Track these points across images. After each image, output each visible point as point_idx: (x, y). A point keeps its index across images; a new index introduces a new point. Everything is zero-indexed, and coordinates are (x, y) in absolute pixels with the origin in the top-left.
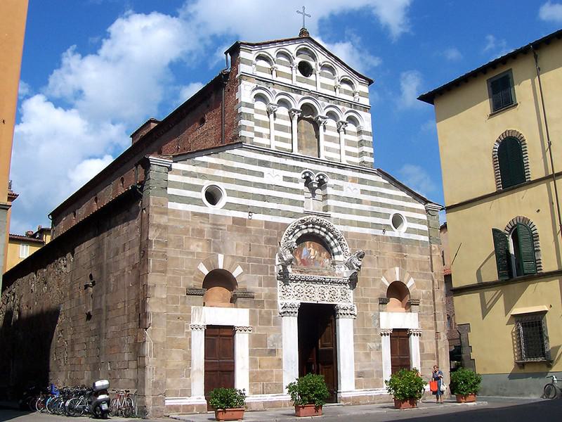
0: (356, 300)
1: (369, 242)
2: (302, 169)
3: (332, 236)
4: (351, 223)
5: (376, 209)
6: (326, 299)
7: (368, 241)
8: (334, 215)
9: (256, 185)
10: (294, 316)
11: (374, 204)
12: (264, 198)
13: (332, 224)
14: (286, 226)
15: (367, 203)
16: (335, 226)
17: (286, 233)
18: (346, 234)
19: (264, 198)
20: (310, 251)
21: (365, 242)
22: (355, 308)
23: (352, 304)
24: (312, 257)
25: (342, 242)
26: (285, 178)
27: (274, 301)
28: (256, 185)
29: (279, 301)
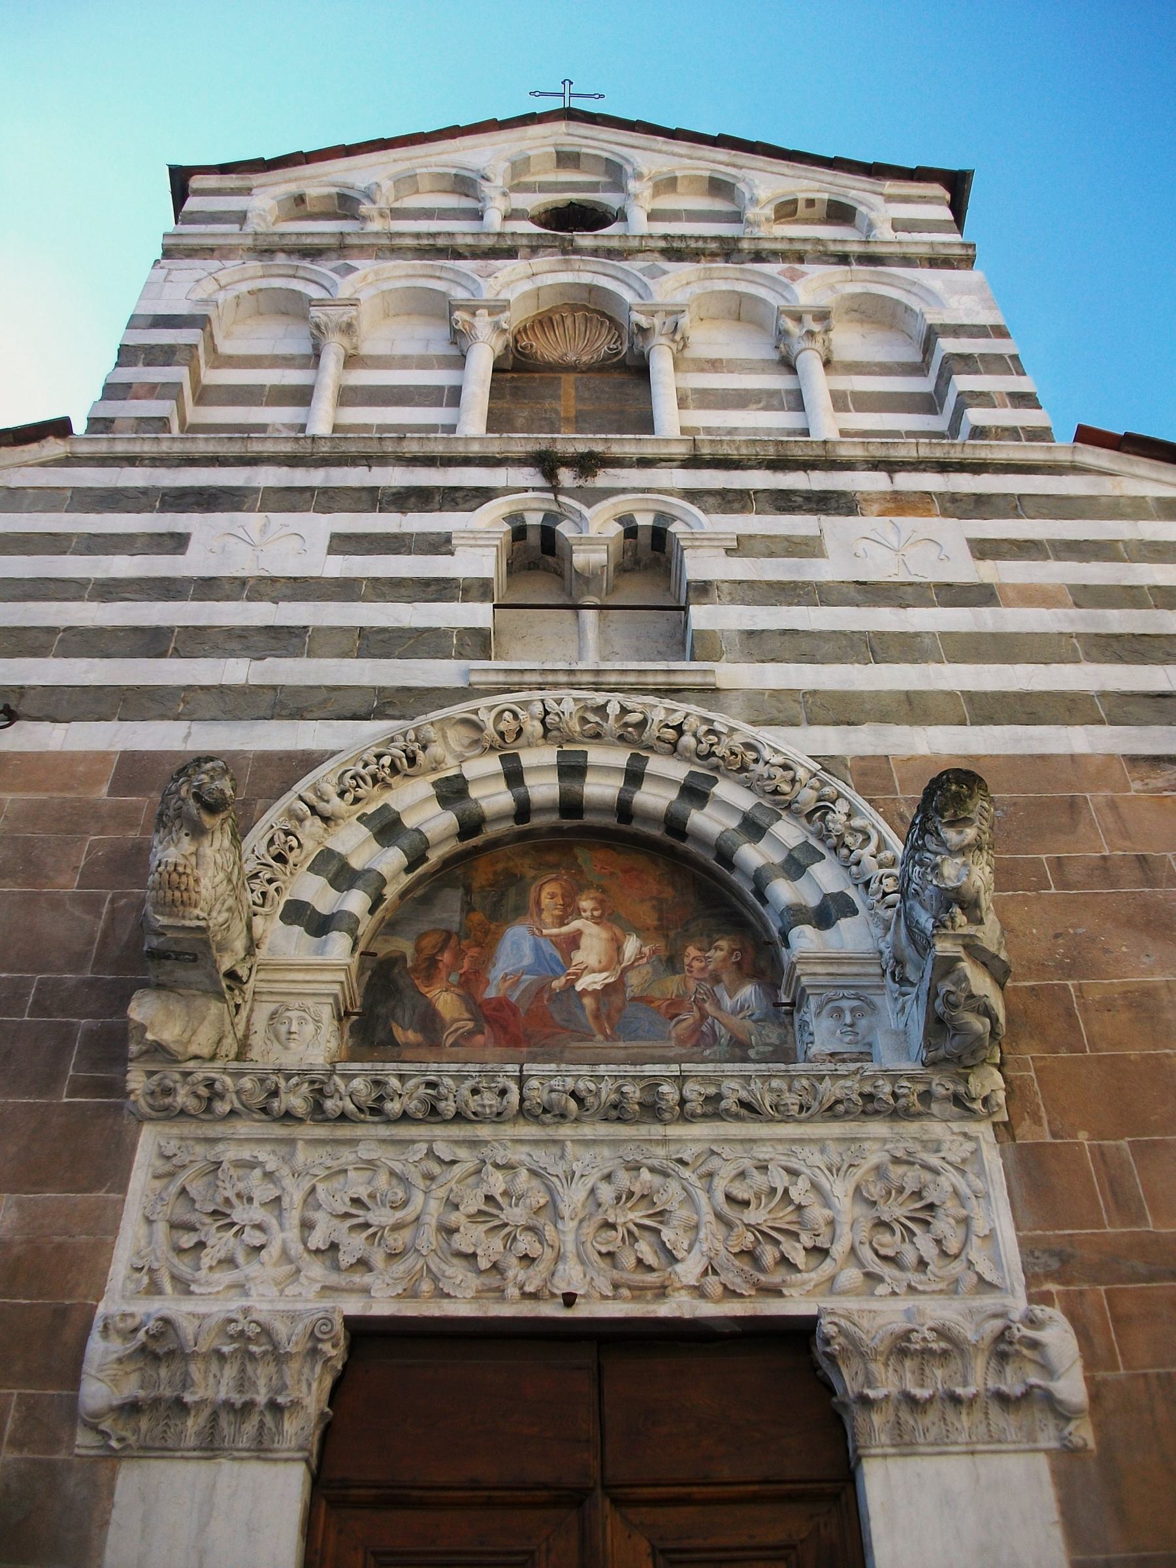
0: (1050, 1265)
1: (1113, 805)
2: (484, 495)
3: (745, 800)
4: (914, 708)
5: (1120, 621)
6: (689, 1270)
7: (1096, 798)
8: (733, 674)
9: (108, 590)
10: (261, 1450)
11: (1088, 596)
12: (153, 642)
13: (721, 721)
14: (308, 761)
15: (1032, 596)
16: (766, 735)
17: (289, 800)
18: (872, 775)
19: (153, 642)
20: (573, 942)
21: (1073, 806)
22: (1059, 1337)
23: (1018, 1304)
24: (590, 982)
25: (837, 819)
26: (342, 544)
27: (62, 1313)
28: (108, 590)
29: (120, 1299)
